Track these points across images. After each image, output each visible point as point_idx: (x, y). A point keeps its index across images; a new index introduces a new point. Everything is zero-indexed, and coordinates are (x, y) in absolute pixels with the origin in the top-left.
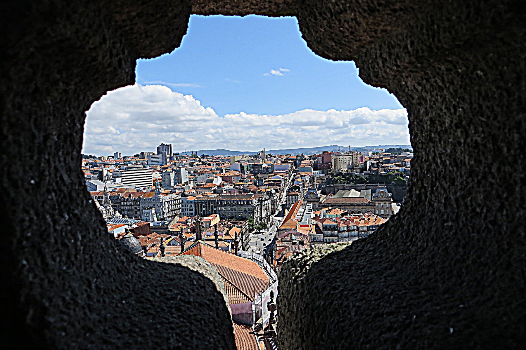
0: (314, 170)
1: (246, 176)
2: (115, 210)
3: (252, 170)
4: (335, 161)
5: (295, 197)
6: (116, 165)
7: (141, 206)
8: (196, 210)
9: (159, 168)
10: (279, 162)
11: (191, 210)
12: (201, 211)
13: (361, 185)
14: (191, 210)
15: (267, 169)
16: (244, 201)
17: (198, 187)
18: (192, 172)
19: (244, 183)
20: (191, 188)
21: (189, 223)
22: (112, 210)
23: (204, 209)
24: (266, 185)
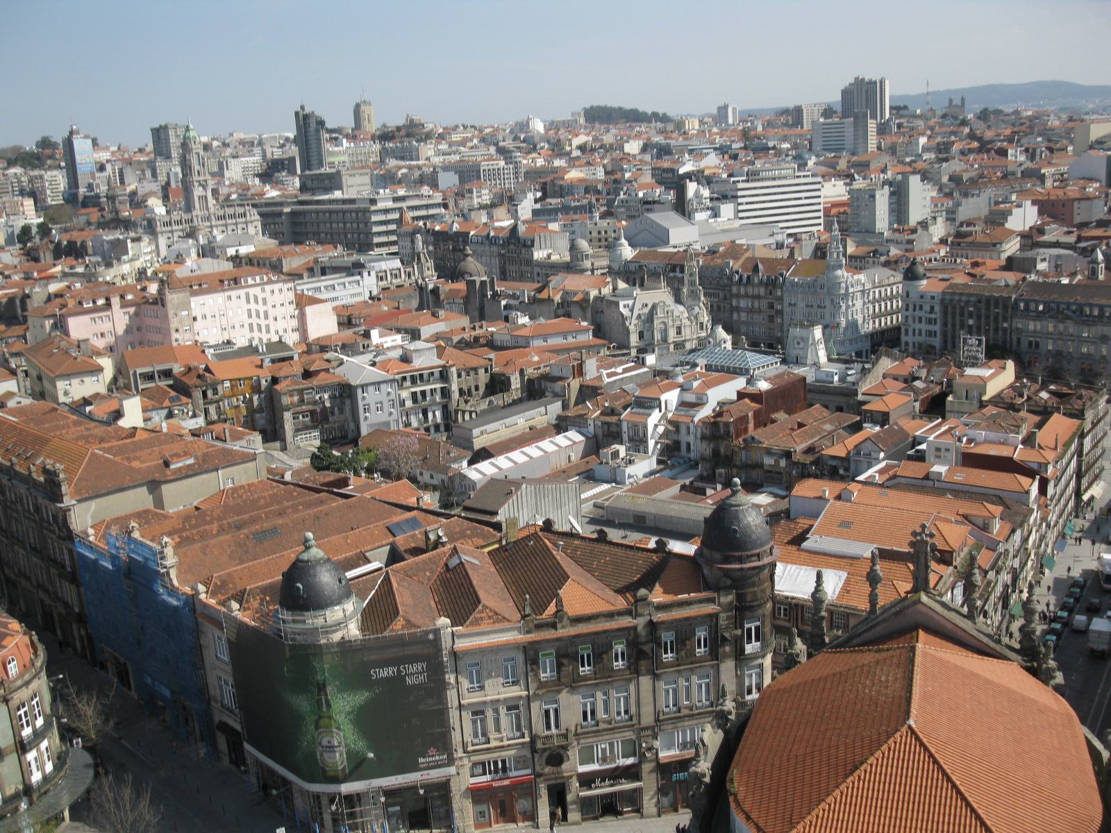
2: (715, 322)
6: (722, 150)
7: (786, 301)
8: (945, 324)
9: (842, 164)
11: (930, 321)
12: (962, 327)
14: (930, 321)
16: (1101, 308)
17: (959, 240)
18: (945, 179)
20: (936, 239)
21: (918, 384)
22: (705, 318)
23: (971, 322)
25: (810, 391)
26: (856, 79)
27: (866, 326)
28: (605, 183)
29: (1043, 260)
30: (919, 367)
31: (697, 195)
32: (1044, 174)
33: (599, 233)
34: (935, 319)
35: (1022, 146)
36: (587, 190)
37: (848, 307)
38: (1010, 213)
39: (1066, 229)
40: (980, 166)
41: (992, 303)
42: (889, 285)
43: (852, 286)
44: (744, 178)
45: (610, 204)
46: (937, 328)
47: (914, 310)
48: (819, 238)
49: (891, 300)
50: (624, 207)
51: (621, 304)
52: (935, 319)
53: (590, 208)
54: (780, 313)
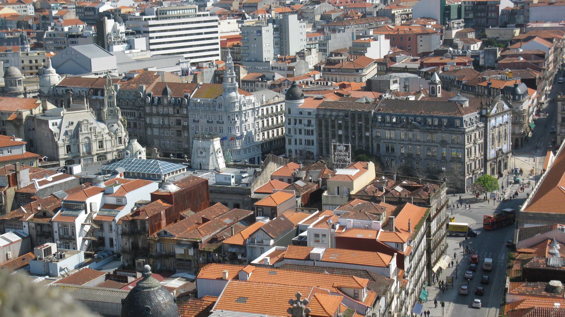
1: (454, 32)
3: (471, 16)
7: (191, 119)
8: (320, 135)
12: (334, 137)
14: (308, 133)
15: (511, 15)
16: (440, 119)
17: (329, 66)
18: (318, 18)
19: (445, 60)
20: (311, 67)
21: (299, 183)
22: (123, 133)
23: (340, 132)
24: (506, 66)
25: (212, 192)
27: (257, 137)
28: (35, 19)
29: (395, 82)
30: (299, 169)
31: (115, 30)
32: (394, 14)
33: (31, 62)
34: (312, 131)
36: (19, 25)
37: (242, 122)
40: (345, 8)
41: (356, 117)
42: (274, 104)
43: (245, 105)
44: (154, 16)
45: (39, 37)
46: (314, 138)
47: (295, 124)
48: (217, 66)
49: (276, 116)
50: (51, 39)
51: (50, 122)
52: (312, 131)
53: (22, 40)
54: (186, 128)
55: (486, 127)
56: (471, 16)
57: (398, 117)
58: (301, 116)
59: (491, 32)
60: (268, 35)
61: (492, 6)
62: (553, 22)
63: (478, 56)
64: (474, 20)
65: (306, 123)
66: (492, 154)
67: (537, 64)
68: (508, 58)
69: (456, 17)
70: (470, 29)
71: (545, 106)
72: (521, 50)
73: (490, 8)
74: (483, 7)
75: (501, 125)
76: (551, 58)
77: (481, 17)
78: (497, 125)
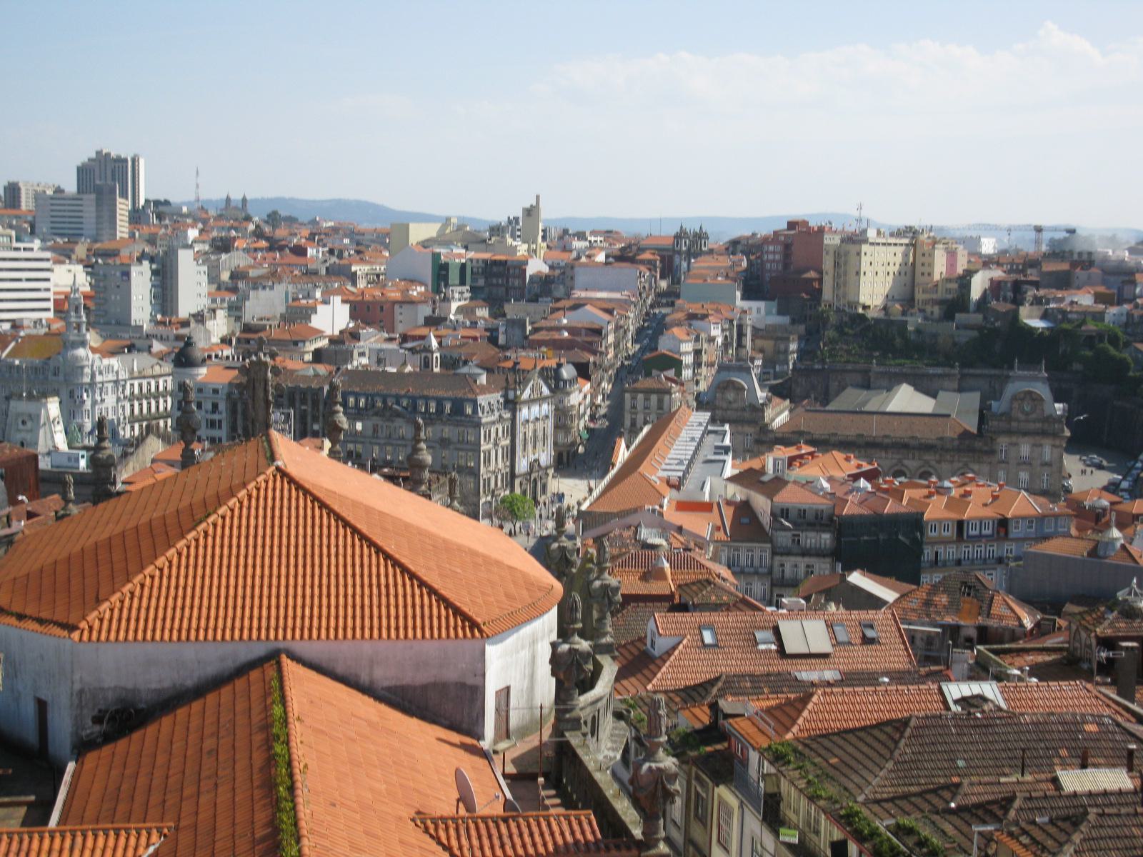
0: (744, 298)
1: (454, 306)
3: (481, 282)
4: (837, 265)
5: (660, 401)
10: (601, 257)
13: (939, 371)
20: (215, 339)
24: (540, 343)
25: (44, 480)
26: (99, 153)
27: (122, 433)
29: (362, 354)
30: (203, 450)
32: (355, 273)
34: (220, 421)
35: (324, 246)
37: (94, 403)
38: (314, 310)
39: (386, 335)
40: (270, 265)
41: (297, 397)
42: (153, 377)
43: (101, 373)
48: (49, 327)
49: (156, 398)
52: (220, 421)
55: (513, 420)
56: (481, 282)
57: (370, 398)
58: (200, 395)
59: (513, 309)
60: (141, 281)
61: (515, 267)
62: (612, 290)
63: (497, 330)
64: (487, 290)
65: (210, 407)
66: (522, 465)
67: (591, 343)
68: (544, 333)
69: (457, 282)
70: (481, 302)
71: (603, 411)
72: (565, 321)
73: (511, 271)
74: (501, 268)
75: (537, 419)
76: (611, 339)
77: (497, 285)
78: (532, 418)
